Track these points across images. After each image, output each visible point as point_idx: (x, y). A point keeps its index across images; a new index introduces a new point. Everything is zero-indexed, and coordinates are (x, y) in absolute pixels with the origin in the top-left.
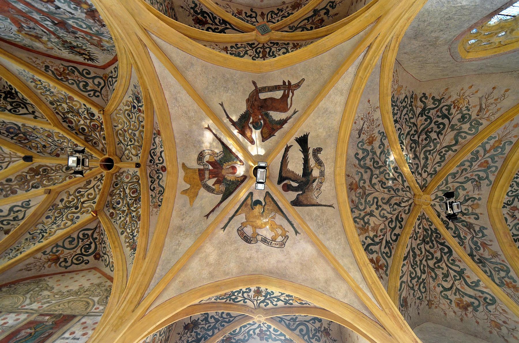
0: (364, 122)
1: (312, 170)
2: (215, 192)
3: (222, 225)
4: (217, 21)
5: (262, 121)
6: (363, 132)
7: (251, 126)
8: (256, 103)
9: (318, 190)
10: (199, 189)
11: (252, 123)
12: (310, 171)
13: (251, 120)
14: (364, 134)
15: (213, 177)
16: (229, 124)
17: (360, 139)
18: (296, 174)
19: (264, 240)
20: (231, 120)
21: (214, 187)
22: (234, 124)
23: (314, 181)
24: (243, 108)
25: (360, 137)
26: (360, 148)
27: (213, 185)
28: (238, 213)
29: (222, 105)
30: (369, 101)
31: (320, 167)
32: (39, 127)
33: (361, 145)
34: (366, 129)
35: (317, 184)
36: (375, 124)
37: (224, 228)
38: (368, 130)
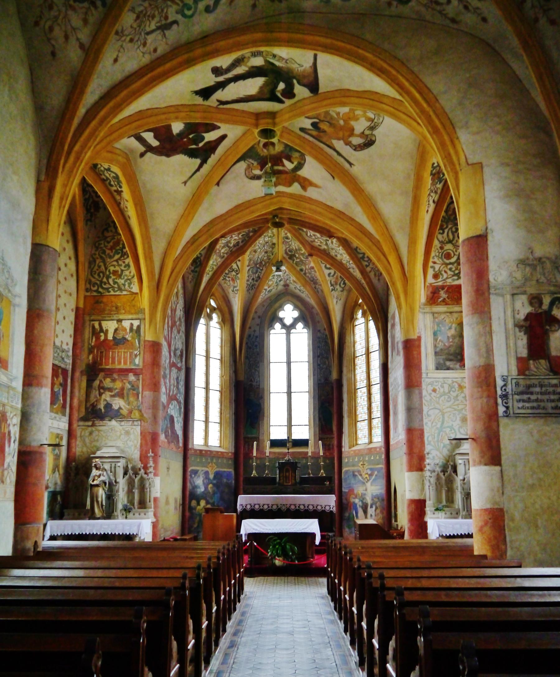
0: (148, 33)
1: (253, 67)
2: (303, 162)
3: (347, 165)
4: (87, 196)
5: (191, 136)
6: (164, 22)
7: (201, 145)
8: (168, 146)
9: (288, 61)
10: (299, 176)
11: (197, 145)
12: (255, 69)
13: (194, 146)
14: (166, 18)
15: (282, 162)
16: (206, 168)
17: (179, 17)
18: (264, 84)
19: (372, 128)
20: (201, 166)
21: (295, 163)
22: (204, 161)
23: (272, 64)
24: (180, 159)
25: (175, 22)
26: (196, 8)
27: (293, 163)
28: (331, 146)
29: (185, 183)
30: (116, 60)
31: (245, 60)
32: (248, 258)
33: (189, 9)
34: (157, 19)
35: (278, 61)
36: (141, 8)
37: (351, 164)
38: (156, 13)
